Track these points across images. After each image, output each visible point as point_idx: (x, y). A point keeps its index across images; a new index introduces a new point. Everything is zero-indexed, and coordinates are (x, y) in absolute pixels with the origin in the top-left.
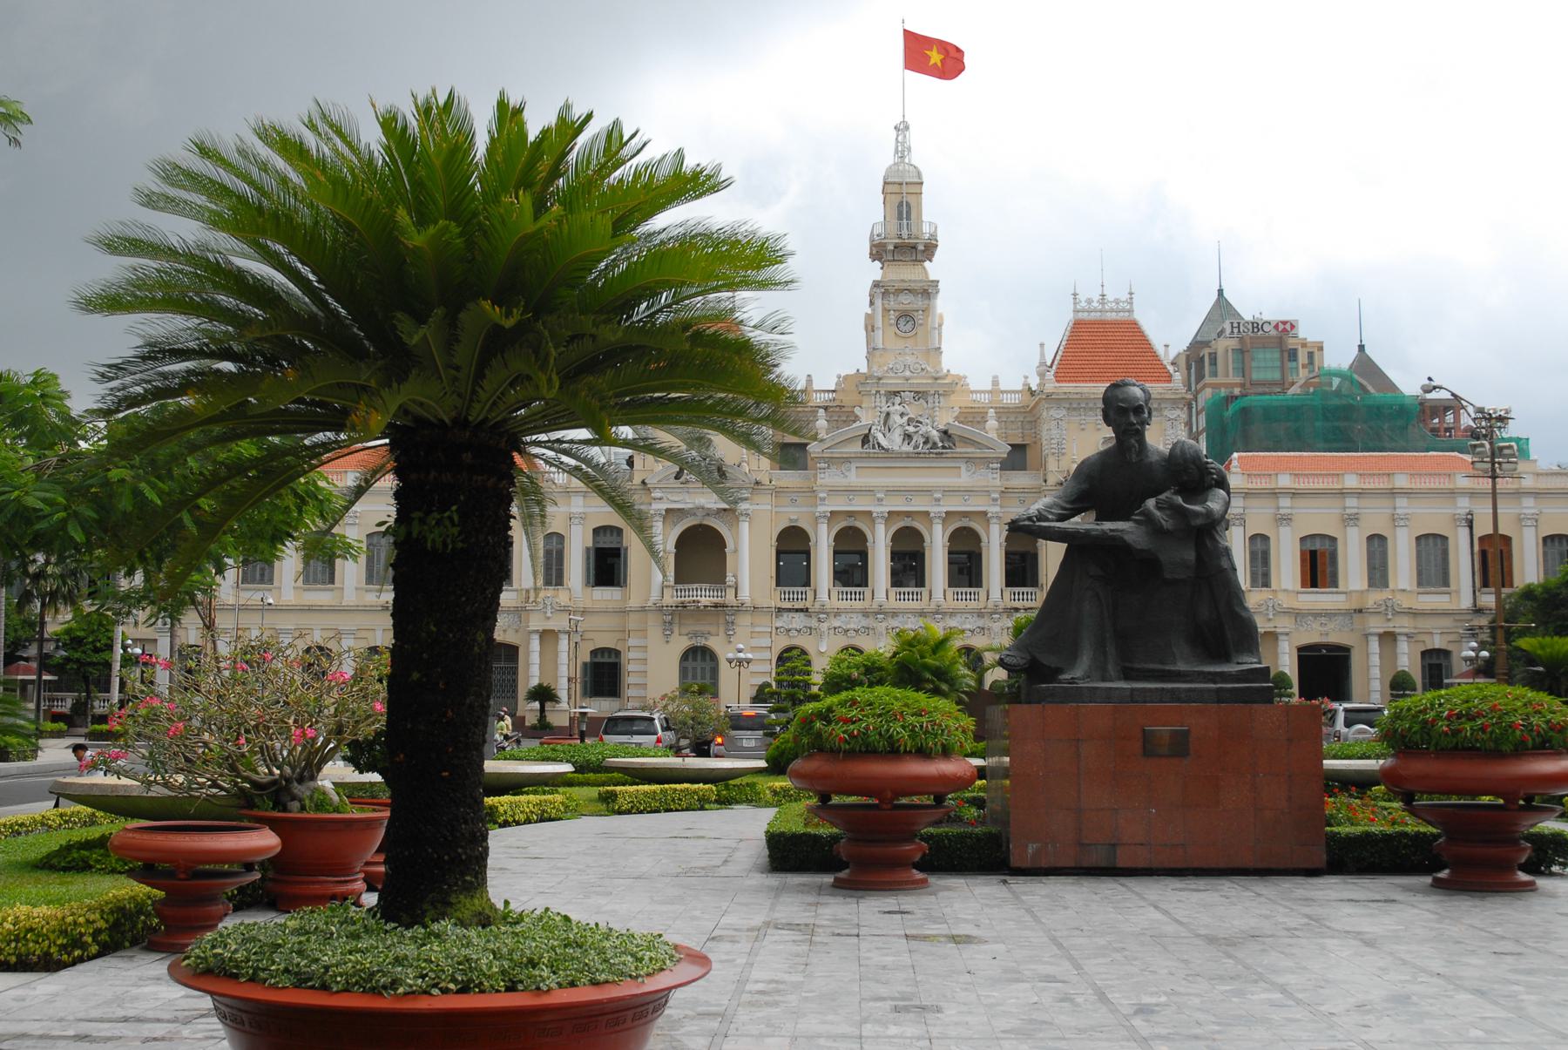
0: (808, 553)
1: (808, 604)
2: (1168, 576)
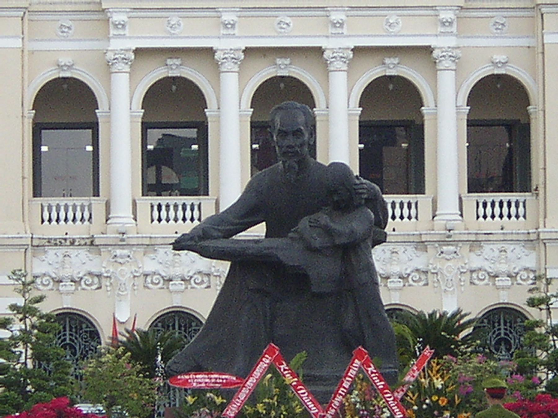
0: (94, 127)
1: (95, 228)
2: (314, 289)
